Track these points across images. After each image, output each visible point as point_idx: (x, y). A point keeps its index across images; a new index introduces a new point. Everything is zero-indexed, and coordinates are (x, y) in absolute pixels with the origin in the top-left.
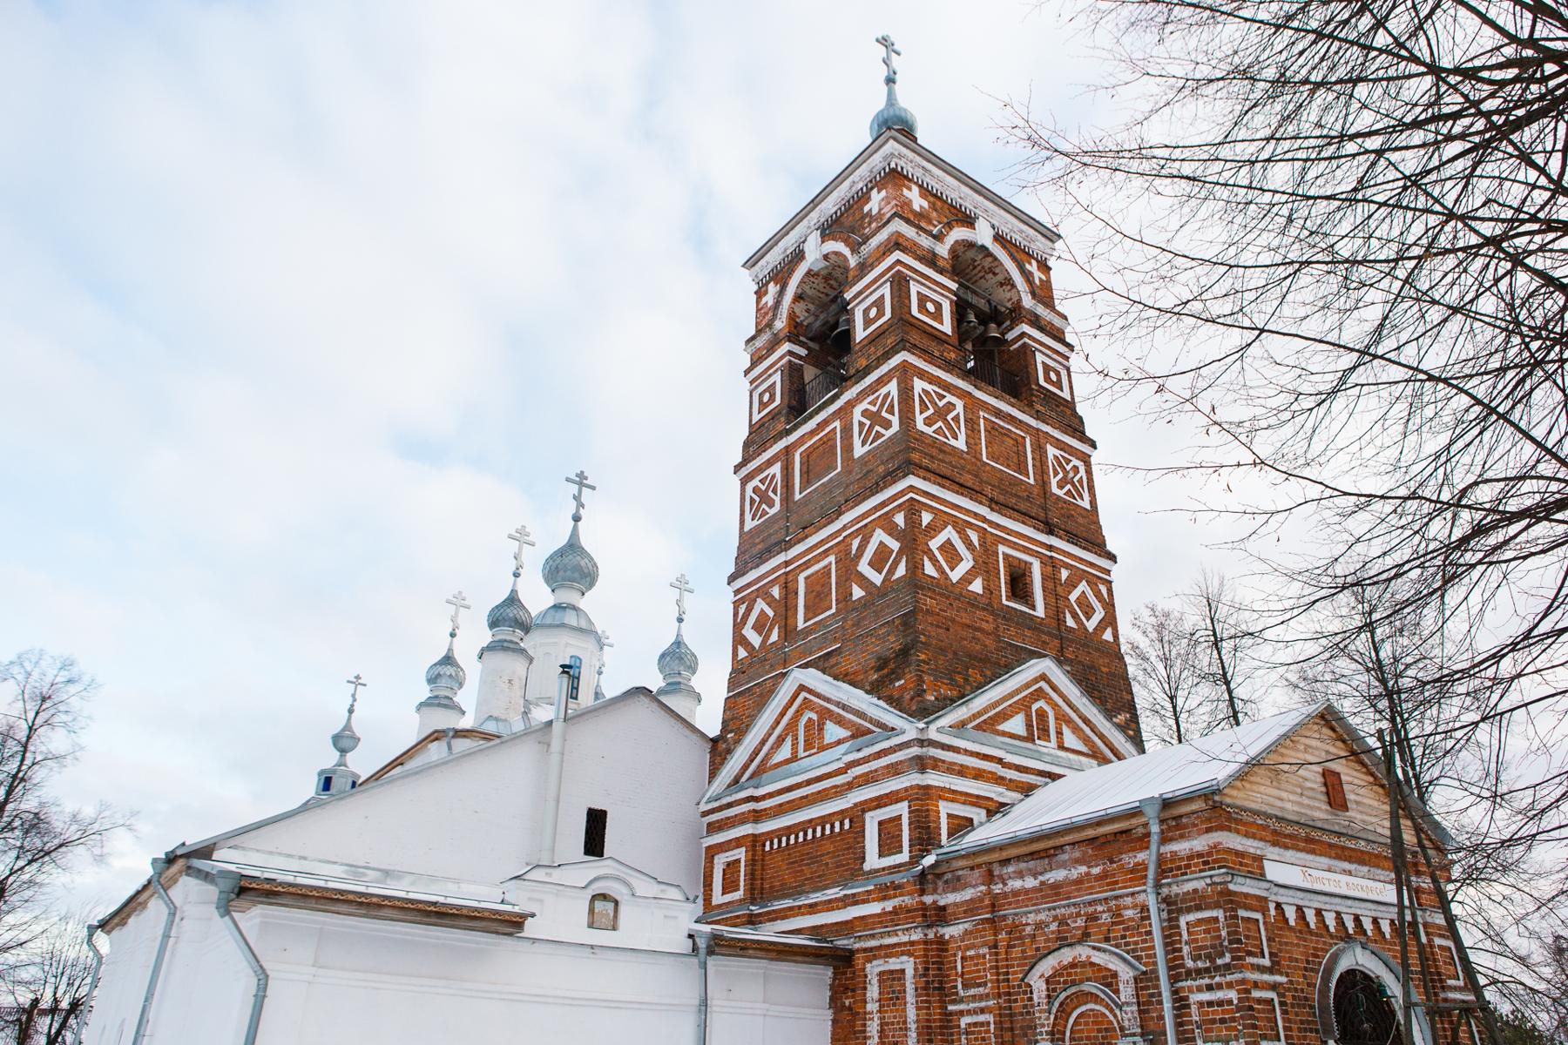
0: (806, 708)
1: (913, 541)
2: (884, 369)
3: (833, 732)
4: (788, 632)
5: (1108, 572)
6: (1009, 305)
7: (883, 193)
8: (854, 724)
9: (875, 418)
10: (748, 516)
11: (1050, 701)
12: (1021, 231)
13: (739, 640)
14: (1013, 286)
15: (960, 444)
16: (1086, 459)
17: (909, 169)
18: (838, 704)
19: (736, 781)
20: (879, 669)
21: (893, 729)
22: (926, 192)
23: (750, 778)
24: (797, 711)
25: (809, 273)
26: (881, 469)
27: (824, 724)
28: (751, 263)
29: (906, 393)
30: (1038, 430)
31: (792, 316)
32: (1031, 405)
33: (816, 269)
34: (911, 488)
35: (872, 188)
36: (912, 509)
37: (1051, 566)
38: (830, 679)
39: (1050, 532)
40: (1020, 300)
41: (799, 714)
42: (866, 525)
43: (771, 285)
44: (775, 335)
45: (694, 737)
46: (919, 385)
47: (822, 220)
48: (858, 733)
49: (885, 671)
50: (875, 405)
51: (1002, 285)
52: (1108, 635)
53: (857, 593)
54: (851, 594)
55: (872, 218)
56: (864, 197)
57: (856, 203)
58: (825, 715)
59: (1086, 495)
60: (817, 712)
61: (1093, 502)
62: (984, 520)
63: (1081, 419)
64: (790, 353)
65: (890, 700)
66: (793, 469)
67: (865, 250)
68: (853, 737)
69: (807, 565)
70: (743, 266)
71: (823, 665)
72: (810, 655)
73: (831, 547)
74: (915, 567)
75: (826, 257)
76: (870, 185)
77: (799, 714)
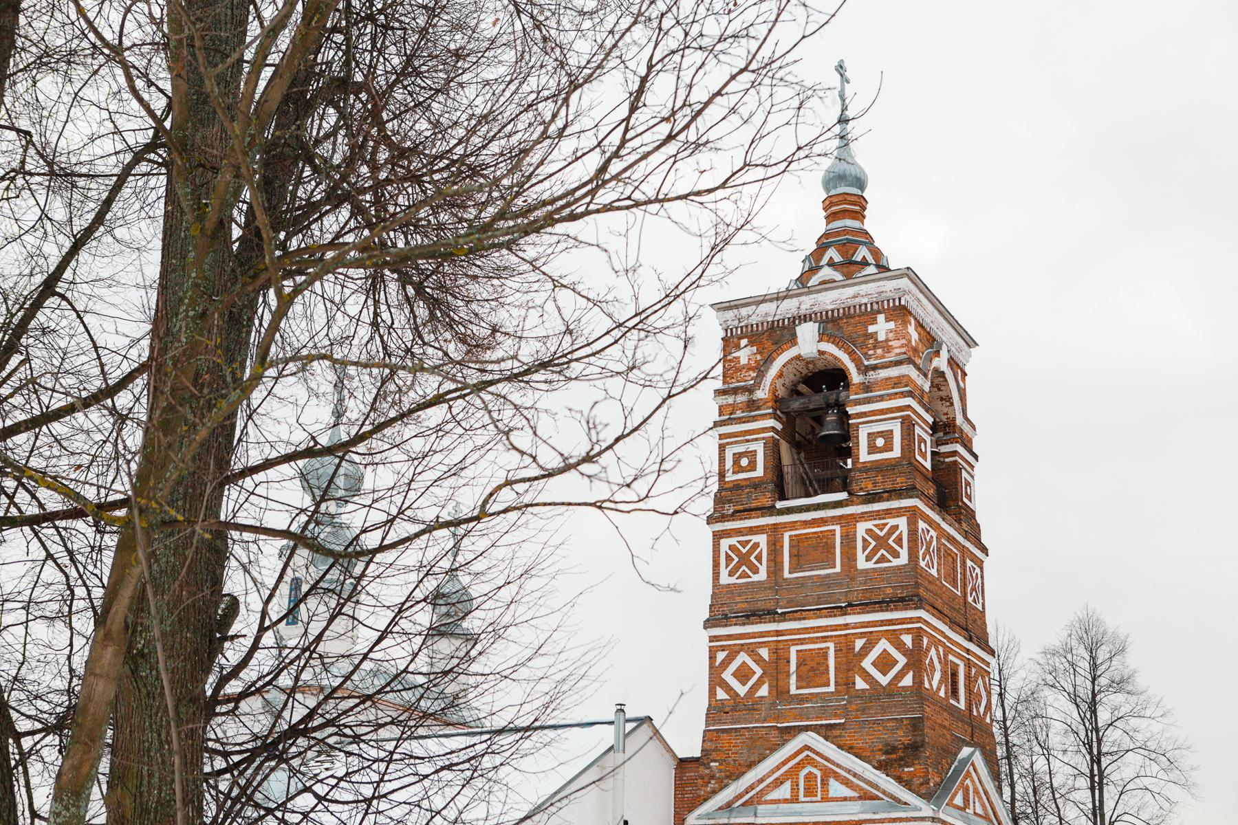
0: (809, 763)
1: (916, 660)
2: (895, 504)
3: (836, 789)
4: (780, 692)
5: (988, 664)
6: (944, 418)
7: (892, 325)
8: (862, 789)
9: (882, 542)
10: (724, 572)
11: (973, 781)
12: (957, 344)
13: (716, 680)
14: (952, 404)
15: (934, 572)
16: (980, 564)
17: (913, 305)
18: (849, 771)
19: (728, 806)
20: (886, 753)
21: (906, 803)
22: (920, 325)
23: (743, 805)
24: (798, 764)
25: (798, 358)
26: (889, 591)
27: (827, 780)
29: (913, 532)
30: (964, 546)
31: (774, 391)
32: (959, 521)
34: (919, 619)
35: (879, 312)
36: (918, 635)
37: (969, 664)
38: (835, 747)
39: (971, 640)
41: (801, 766)
42: (871, 632)
45: (668, 756)
46: (922, 525)
47: (816, 309)
48: (865, 796)
49: (894, 756)
50: (881, 530)
51: (942, 399)
52: (988, 720)
53: (860, 684)
54: (854, 683)
56: (871, 317)
57: (859, 316)
58: (828, 774)
59: (981, 601)
60: (821, 770)
61: (983, 605)
62: (946, 637)
63: (978, 526)
64: (773, 429)
65: (899, 779)
66: (782, 547)
67: (872, 375)
68: (860, 798)
69: (802, 641)
70: (712, 306)
71: (826, 732)
72: (808, 719)
73: (831, 636)
74: (918, 681)
75: (821, 353)
77: (801, 766)
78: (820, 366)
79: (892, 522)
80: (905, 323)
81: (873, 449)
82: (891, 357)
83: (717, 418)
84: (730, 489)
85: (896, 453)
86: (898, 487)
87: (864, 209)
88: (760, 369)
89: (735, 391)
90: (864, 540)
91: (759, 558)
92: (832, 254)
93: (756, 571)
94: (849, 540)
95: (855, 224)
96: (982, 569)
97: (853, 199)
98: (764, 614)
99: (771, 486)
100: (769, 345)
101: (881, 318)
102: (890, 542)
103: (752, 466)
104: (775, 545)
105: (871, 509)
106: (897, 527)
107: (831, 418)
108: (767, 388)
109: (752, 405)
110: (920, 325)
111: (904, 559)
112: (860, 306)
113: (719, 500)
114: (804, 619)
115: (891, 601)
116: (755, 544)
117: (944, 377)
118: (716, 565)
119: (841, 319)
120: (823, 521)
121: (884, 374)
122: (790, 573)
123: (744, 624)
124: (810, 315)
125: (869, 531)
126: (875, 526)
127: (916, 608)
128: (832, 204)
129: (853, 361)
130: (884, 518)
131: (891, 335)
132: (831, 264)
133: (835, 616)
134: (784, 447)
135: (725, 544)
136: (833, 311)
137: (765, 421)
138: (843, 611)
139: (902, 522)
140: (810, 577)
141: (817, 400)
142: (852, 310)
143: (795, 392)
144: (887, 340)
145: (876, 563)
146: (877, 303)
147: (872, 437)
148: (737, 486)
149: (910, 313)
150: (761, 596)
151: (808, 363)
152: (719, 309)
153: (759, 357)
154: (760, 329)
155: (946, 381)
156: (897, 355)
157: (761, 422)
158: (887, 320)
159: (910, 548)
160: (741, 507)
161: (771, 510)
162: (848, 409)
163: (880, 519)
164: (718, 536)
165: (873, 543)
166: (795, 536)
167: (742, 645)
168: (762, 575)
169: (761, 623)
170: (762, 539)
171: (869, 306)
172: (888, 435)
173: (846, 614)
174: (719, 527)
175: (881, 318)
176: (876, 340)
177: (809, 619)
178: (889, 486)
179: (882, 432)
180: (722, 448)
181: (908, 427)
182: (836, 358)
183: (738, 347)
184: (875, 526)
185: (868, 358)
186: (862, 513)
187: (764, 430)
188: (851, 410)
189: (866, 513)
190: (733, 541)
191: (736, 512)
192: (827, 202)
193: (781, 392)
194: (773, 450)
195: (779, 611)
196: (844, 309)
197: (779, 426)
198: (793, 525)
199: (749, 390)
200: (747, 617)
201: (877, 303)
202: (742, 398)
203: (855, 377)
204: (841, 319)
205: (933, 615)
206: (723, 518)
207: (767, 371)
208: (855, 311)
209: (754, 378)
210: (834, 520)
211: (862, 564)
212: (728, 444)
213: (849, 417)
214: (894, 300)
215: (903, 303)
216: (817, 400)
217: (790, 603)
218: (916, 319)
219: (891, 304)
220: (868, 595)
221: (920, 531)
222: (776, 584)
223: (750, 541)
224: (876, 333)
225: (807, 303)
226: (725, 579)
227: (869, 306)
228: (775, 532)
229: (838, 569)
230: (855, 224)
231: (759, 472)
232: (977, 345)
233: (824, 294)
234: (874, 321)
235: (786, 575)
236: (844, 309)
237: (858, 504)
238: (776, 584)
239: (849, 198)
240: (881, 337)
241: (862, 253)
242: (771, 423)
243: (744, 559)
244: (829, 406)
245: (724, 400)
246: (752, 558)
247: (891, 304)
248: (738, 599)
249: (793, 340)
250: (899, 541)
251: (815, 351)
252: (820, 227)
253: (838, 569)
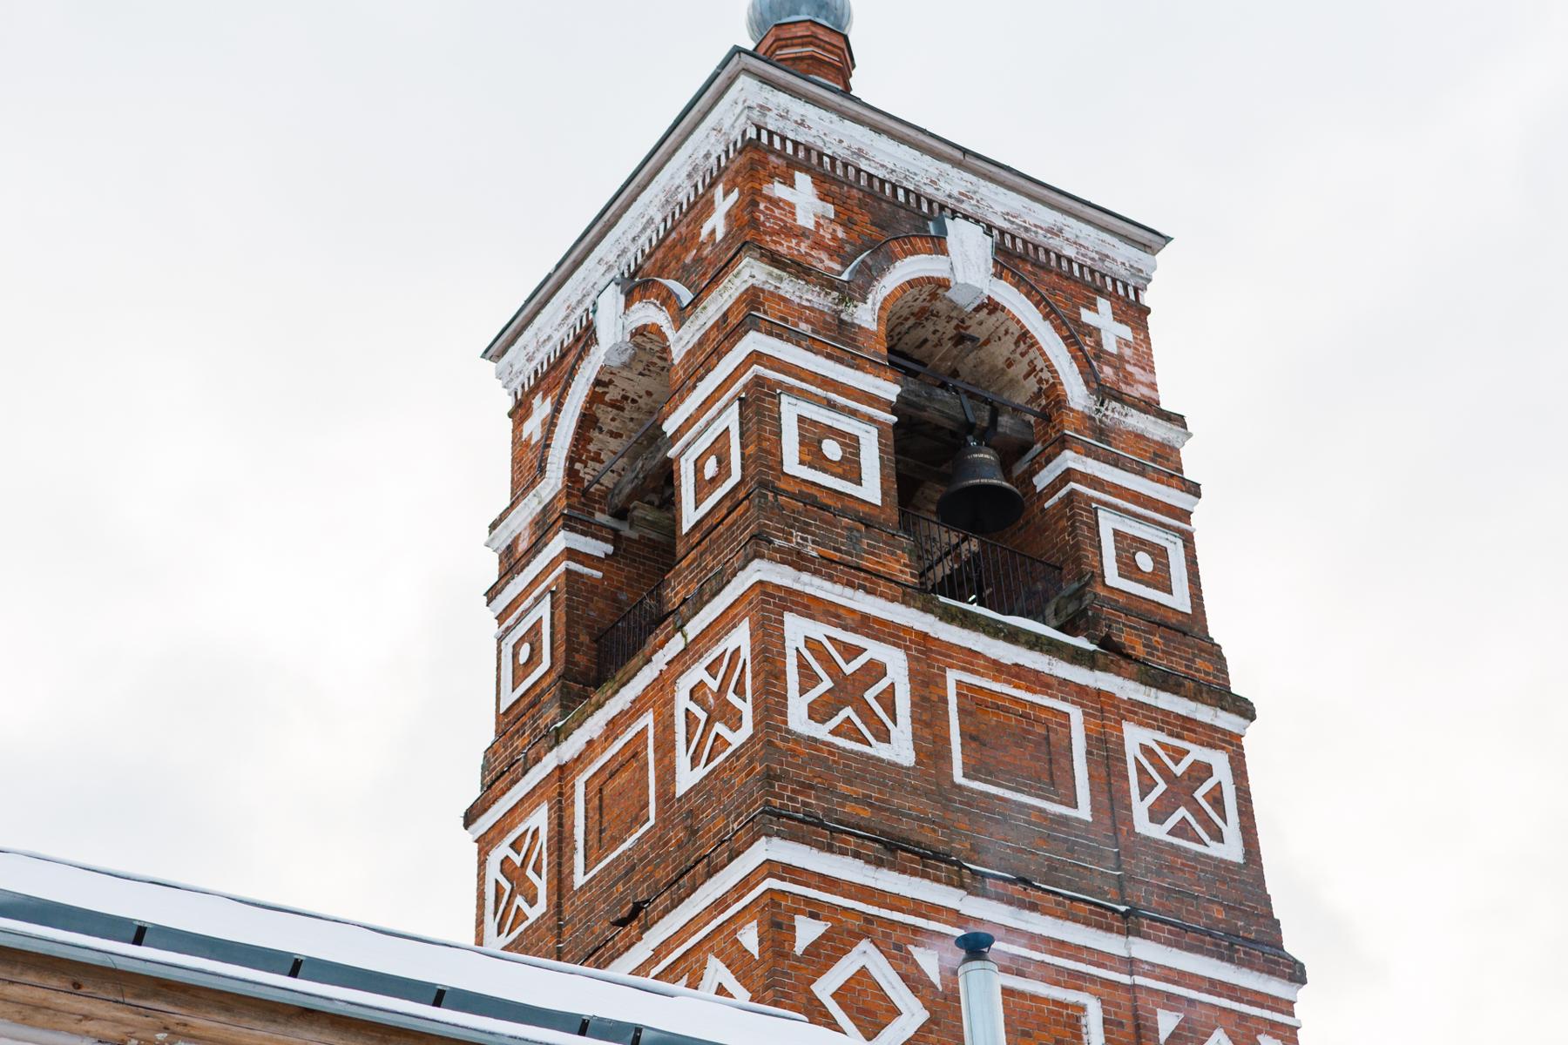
44: (842, 322)
114: (1033, 907)
123: (879, 863)
137: (880, 382)
157: (870, 379)
163: (1171, 734)
167: (869, 919)
169: (925, 875)
177: (1045, 912)
189: (1143, 705)
210: (1080, 694)
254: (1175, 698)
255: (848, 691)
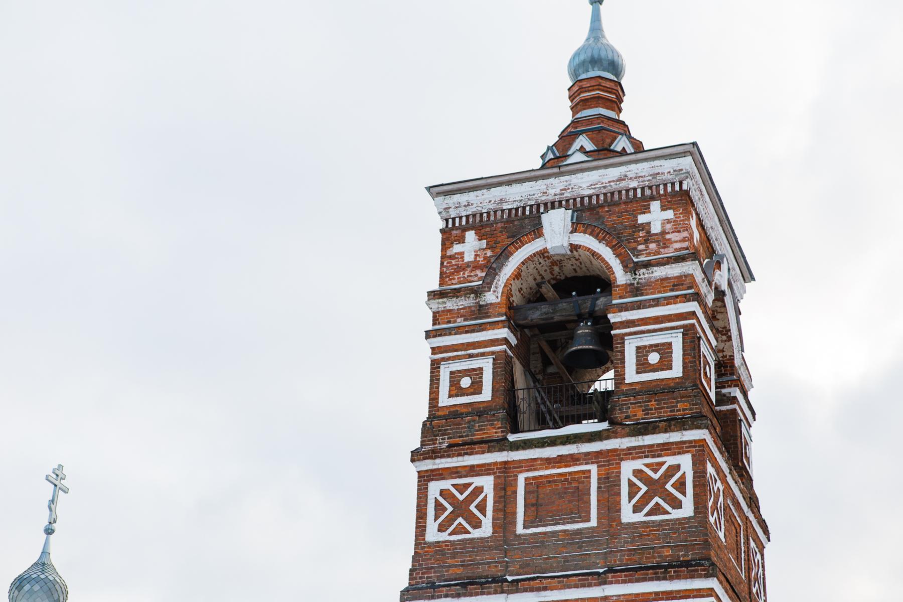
2: (675, 437)
7: (670, 214)
10: (432, 527)
14: (730, 338)
16: (761, 548)
17: (695, 195)
22: (701, 224)
25: (543, 253)
26: (667, 552)
28: (438, 191)
31: (508, 294)
33: (552, 252)
35: (653, 198)
40: (732, 358)
43: (470, 236)
44: (481, 306)
47: (567, 195)
50: (655, 471)
55: (649, 238)
57: (625, 203)
64: (506, 341)
66: (515, 492)
67: (644, 275)
70: (429, 189)
75: (574, 247)
76: (648, 192)
78: (568, 270)
79: (671, 461)
80: (687, 214)
81: (643, 366)
82: (669, 252)
83: (430, 327)
84: (445, 417)
85: (677, 371)
86: (679, 415)
87: (621, 101)
88: (491, 268)
89: (456, 293)
90: (631, 484)
91: (482, 508)
92: (583, 141)
93: (477, 524)
94: (609, 484)
95: (611, 114)
96: (762, 555)
97: (608, 84)
98: (487, 582)
99: (501, 414)
100: (504, 239)
101: (655, 205)
102: (669, 487)
103: (476, 388)
104: (505, 489)
105: (640, 443)
106: (678, 467)
107: (584, 329)
108: (500, 290)
109: (481, 311)
110: (701, 224)
111: (687, 509)
112: (627, 191)
113: (429, 430)
114: (545, 589)
115: (670, 566)
116: (476, 488)
117: (723, 301)
118: (421, 516)
119: (602, 206)
120: (573, 459)
121: (659, 272)
122: (525, 527)
124: (560, 202)
125: (638, 473)
126: (647, 465)
127: (707, 576)
128: (582, 90)
129: (618, 256)
130: (659, 456)
131: (668, 227)
132: (582, 149)
133: (590, 585)
134: (518, 369)
135: (435, 488)
136: (590, 197)
137: (496, 331)
138: (601, 580)
139: (686, 462)
140: (554, 533)
141: (564, 308)
142: (616, 197)
143: (536, 297)
144: (664, 233)
145: (647, 515)
146: (650, 188)
147: (642, 352)
148: (454, 414)
149: (693, 206)
150: (484, 557)
151: (554, 263)
152: (439, 194)
153: (489, 253)
154: (492, 218)
155: (725, 306)
156: (676, 250)
157: (490, 332)
158: (664, 208)
159: (696, 496)
160: (459, 440)
161: (502, 444)
162: (609, 316)
163: (653, 457)
164: (425, 478)
165: (644, 489)
166: (534, 478)
168: (486, 530)
169: (483, 594)
170: (487, 483)
171: (639, 191)
172: (665, 350)
173: (605, 583)
174: (428, 465)
175: (655, 205)
176: (649, 232)
177: (552, 589)
178: (666, 414)
179: (656, 345)
180: (435, 366)
181: (692, 340)
182: (594, 254)
183: (461, 240)
184: (647, 465)
185: (638, 253)
186: (629, 449)
187: (494, 342)
188: (613, 318)
189: (635, 448)
190: (446, 484)
191: (450, 446)
192: (576, 88)
193: (516, 299)
194: (503, 366)
195: (510, 578)
196: (605, 194)
197: (513, 341)
198: (531, 464)
199: (477, 292)
200: (464, 585)
201: (650, 188)
202: (466, 302)
203: (621, 277)
204: (602, 206)
205: (726, 592)
206: (434, 454)
207: (500, 268)
208: (620, 198)
209: (483, 279)
210: (588, 457)
211: (628, 515)
212: (443, 359)
213: (611, 326)
214: (673, 184)
215: (685, 187)
216: (564, 308)
217: (525, 567)
218: (697, 214)
219: (669, 189)
220: (637, 558)
221: (708, 475)
222: (506, 542)
223: (470, 484)
224: (649, 224)
225: (555, 187)
226: (432, 534)
227: (639, 191)
228: (505, 473)
229: (593, 523)
230: (611, 114)
231: (486, 395)
232: (753, 279)
233: (579, 175)
234: (646, 210)
235: (520, 530)
236: (605, 194)
237: (623, 436)
238: (506, 542)
239: (604, 83)
240: (656, 229)
241: (621, 144)
242: (503, 333)
243: (461, 509)
244: (581, 318)
245: (438, 305)
246: (472, 507)
247: (669, 189)
248: (450, 562)
249: (537, 231)
250: (681, 486)
251: (566, 244)
252: (564, 117)
253: (593, 523)
254: (655, 436)
255: (461, 509)
